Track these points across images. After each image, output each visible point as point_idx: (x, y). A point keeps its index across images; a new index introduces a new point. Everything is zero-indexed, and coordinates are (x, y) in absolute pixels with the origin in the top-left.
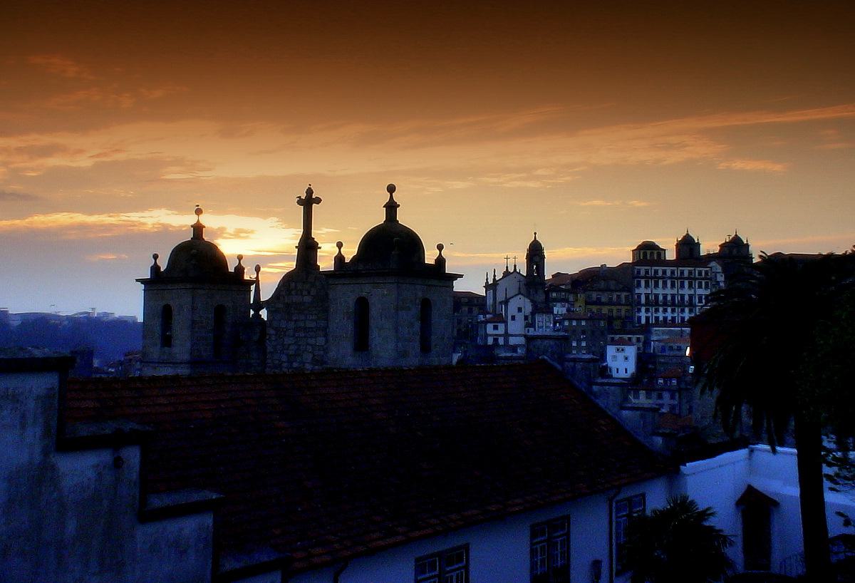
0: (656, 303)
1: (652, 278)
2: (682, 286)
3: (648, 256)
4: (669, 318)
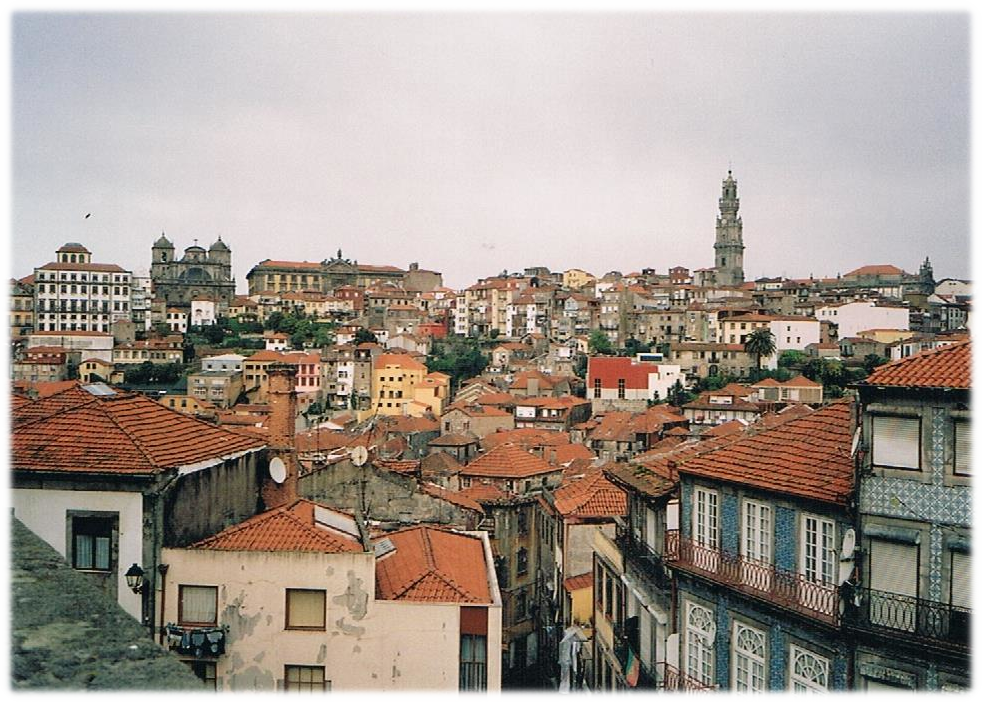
0: (64, 310)
1: (58, 283)
2: (95, 291)
3: (69, 260)
4: (79, 325)
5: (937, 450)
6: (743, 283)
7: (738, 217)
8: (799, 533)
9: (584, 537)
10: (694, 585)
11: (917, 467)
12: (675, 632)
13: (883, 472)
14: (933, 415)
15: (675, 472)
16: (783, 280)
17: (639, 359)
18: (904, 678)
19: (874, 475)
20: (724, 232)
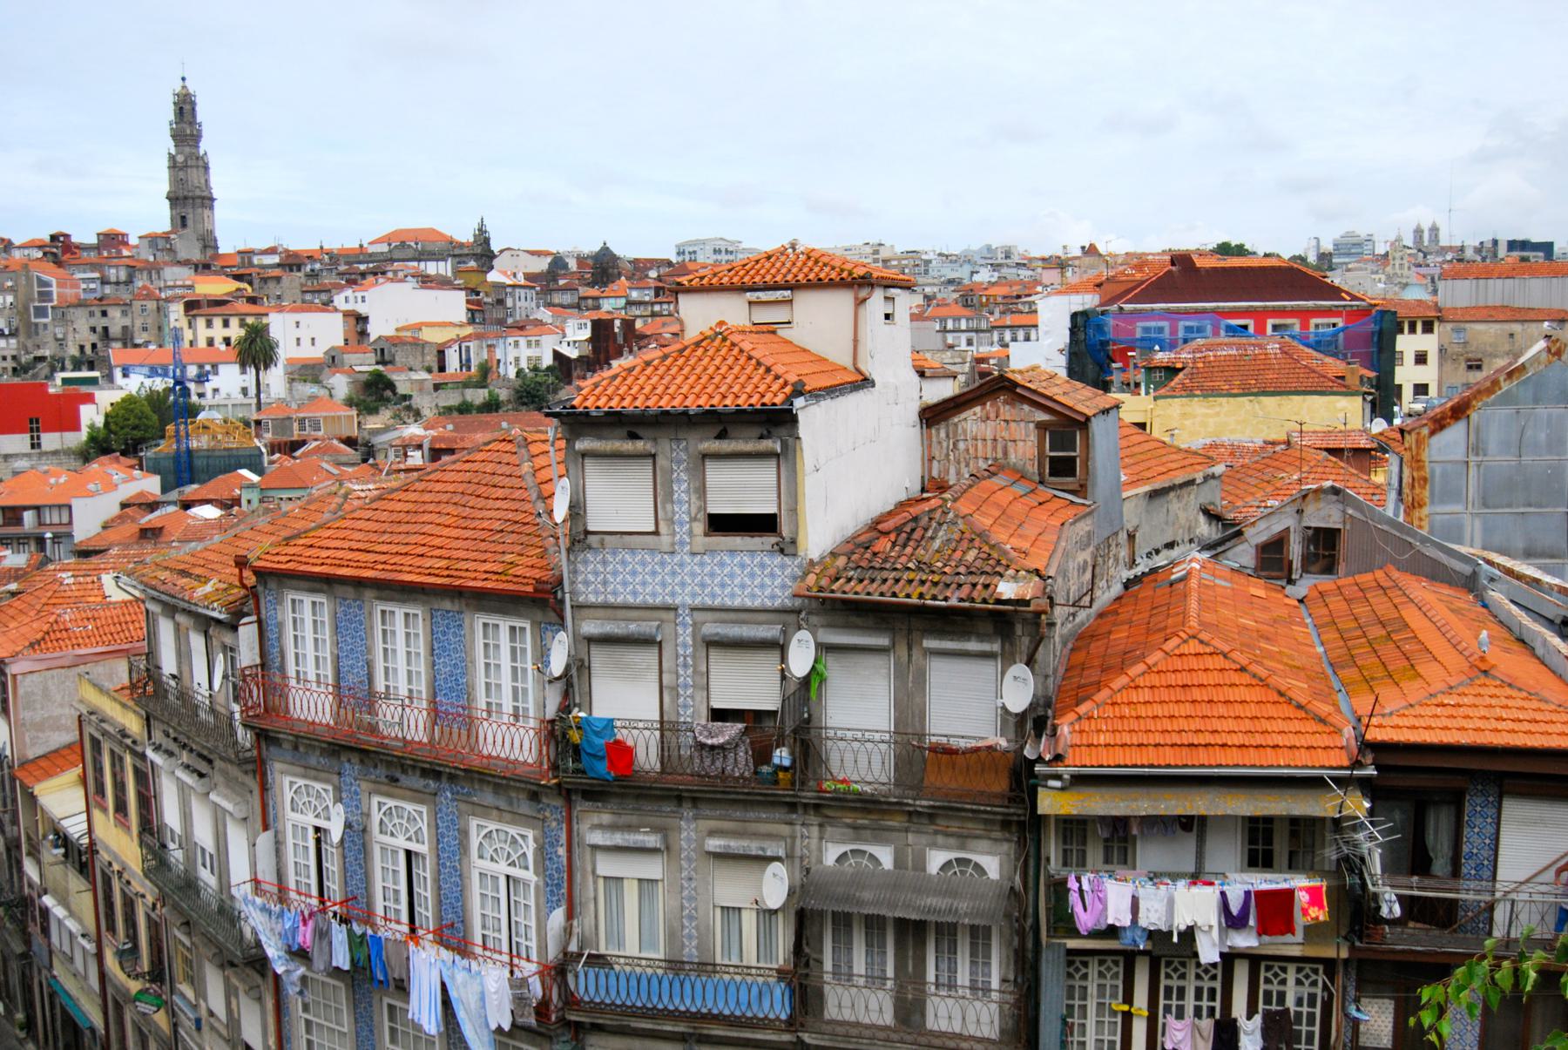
5: (680, 502)
6: (217, 256)
8: (473, 648)
9: (45, 689)
10: (296, 748)
11: (652, 528)
12: (266, 828)
13: (602, 543)
14: (672, 450)
15: (247, 573)
17: (59, 382)
18: (652, 840)
19: (590, 547)
20: (181, 175)
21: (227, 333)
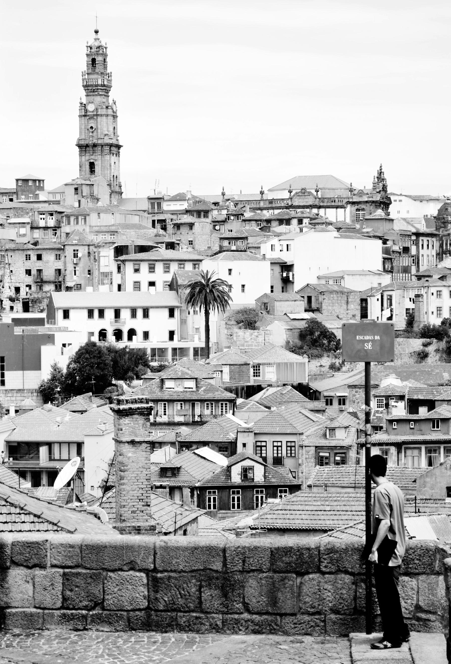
7: (111, 102)
16: (189, 196)
20: (92, 123)
21: (152, 277)
